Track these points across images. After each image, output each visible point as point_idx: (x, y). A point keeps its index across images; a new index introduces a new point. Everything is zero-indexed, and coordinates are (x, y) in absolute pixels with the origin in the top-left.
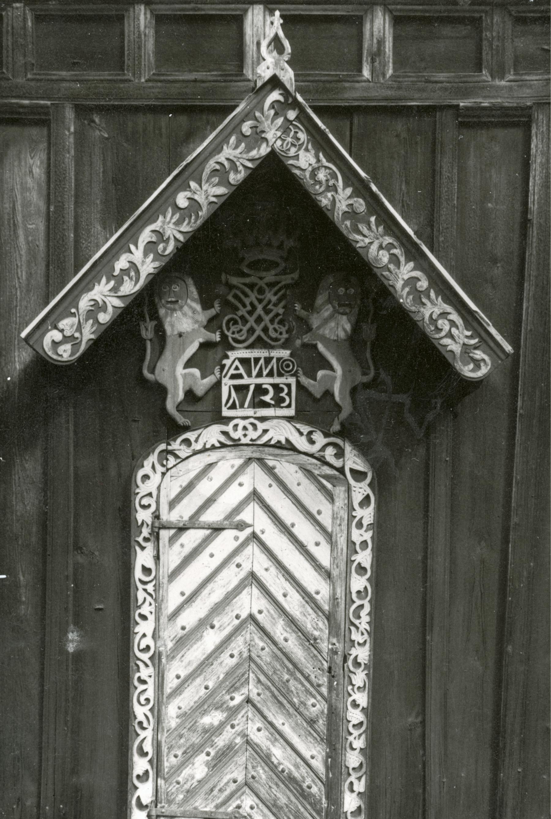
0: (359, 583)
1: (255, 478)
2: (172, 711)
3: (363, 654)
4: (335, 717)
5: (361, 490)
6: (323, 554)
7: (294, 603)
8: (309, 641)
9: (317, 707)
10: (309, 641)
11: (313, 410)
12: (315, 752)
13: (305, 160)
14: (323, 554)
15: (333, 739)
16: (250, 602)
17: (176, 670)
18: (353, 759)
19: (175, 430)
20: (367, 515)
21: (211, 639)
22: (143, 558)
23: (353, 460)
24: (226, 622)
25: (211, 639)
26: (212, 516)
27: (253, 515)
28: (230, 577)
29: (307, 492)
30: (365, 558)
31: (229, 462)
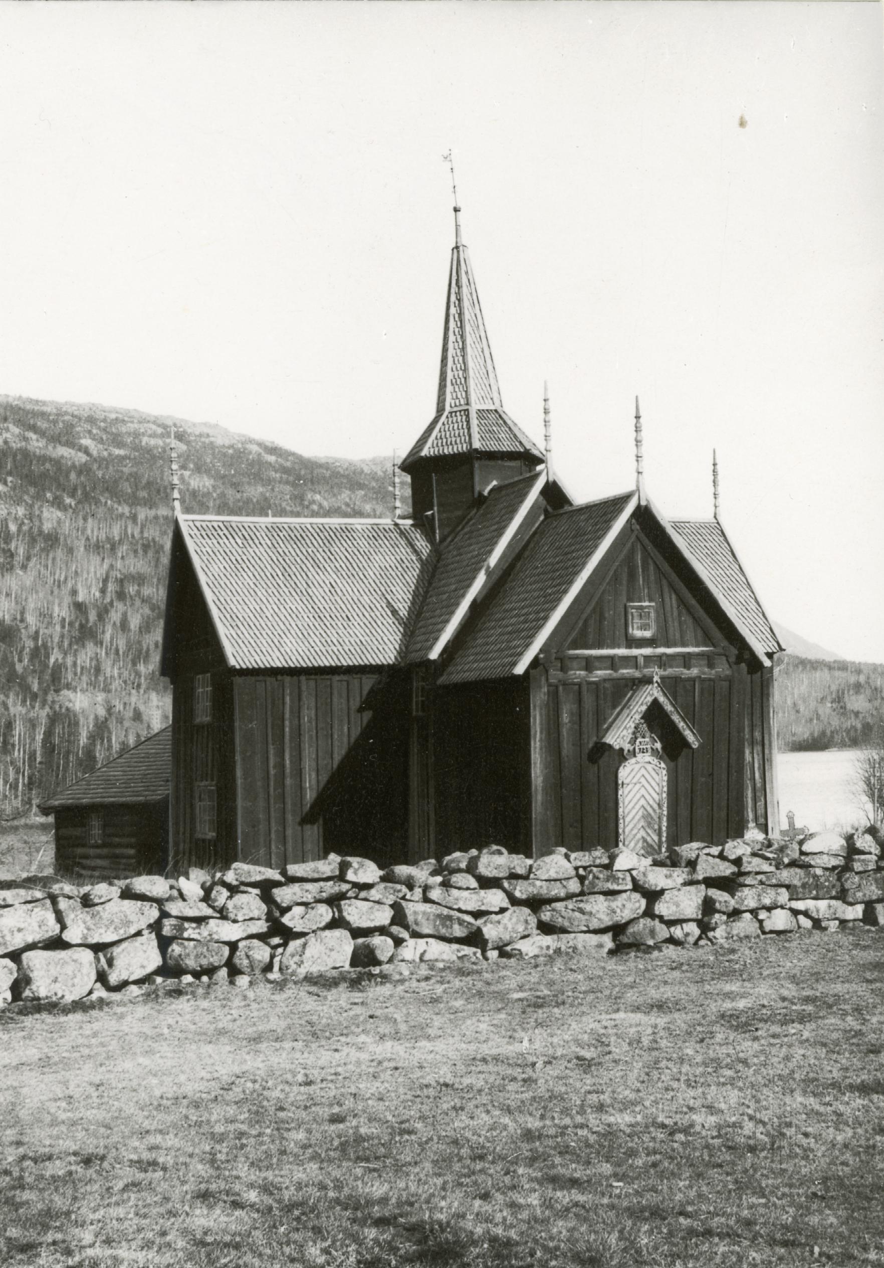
0: (665, 795)
1: (643, 771)
2: (627, 830)
3: (665, 813)
4: (660, 828)
5: (665, 772)
6: (657, 789)
7: (651, 802)
8: (654, 810)
9: (656, 827)
10: (654, 810)
11: (654, 752)
12: (656, 838)
13: (662, 699)
14: (657, 789)
15: (660, 835)
16: (642, 802)
17: (627, 819)
18: (664, 839)
19: (626, 759)
20: (665, 778)
21: (634, 812)
22: (620, 792)
23: (663, 765)
24: (638, 807)
25: (634, 812)
26: (635, 781)
27: (643, 780)
28: (638, 796)
29: (653, 773)
30: (665, 789)
31: (637, 767)
